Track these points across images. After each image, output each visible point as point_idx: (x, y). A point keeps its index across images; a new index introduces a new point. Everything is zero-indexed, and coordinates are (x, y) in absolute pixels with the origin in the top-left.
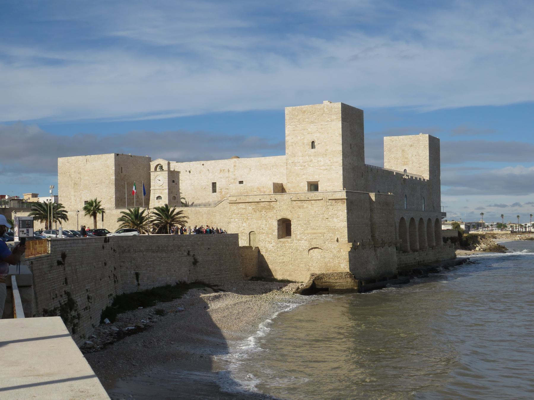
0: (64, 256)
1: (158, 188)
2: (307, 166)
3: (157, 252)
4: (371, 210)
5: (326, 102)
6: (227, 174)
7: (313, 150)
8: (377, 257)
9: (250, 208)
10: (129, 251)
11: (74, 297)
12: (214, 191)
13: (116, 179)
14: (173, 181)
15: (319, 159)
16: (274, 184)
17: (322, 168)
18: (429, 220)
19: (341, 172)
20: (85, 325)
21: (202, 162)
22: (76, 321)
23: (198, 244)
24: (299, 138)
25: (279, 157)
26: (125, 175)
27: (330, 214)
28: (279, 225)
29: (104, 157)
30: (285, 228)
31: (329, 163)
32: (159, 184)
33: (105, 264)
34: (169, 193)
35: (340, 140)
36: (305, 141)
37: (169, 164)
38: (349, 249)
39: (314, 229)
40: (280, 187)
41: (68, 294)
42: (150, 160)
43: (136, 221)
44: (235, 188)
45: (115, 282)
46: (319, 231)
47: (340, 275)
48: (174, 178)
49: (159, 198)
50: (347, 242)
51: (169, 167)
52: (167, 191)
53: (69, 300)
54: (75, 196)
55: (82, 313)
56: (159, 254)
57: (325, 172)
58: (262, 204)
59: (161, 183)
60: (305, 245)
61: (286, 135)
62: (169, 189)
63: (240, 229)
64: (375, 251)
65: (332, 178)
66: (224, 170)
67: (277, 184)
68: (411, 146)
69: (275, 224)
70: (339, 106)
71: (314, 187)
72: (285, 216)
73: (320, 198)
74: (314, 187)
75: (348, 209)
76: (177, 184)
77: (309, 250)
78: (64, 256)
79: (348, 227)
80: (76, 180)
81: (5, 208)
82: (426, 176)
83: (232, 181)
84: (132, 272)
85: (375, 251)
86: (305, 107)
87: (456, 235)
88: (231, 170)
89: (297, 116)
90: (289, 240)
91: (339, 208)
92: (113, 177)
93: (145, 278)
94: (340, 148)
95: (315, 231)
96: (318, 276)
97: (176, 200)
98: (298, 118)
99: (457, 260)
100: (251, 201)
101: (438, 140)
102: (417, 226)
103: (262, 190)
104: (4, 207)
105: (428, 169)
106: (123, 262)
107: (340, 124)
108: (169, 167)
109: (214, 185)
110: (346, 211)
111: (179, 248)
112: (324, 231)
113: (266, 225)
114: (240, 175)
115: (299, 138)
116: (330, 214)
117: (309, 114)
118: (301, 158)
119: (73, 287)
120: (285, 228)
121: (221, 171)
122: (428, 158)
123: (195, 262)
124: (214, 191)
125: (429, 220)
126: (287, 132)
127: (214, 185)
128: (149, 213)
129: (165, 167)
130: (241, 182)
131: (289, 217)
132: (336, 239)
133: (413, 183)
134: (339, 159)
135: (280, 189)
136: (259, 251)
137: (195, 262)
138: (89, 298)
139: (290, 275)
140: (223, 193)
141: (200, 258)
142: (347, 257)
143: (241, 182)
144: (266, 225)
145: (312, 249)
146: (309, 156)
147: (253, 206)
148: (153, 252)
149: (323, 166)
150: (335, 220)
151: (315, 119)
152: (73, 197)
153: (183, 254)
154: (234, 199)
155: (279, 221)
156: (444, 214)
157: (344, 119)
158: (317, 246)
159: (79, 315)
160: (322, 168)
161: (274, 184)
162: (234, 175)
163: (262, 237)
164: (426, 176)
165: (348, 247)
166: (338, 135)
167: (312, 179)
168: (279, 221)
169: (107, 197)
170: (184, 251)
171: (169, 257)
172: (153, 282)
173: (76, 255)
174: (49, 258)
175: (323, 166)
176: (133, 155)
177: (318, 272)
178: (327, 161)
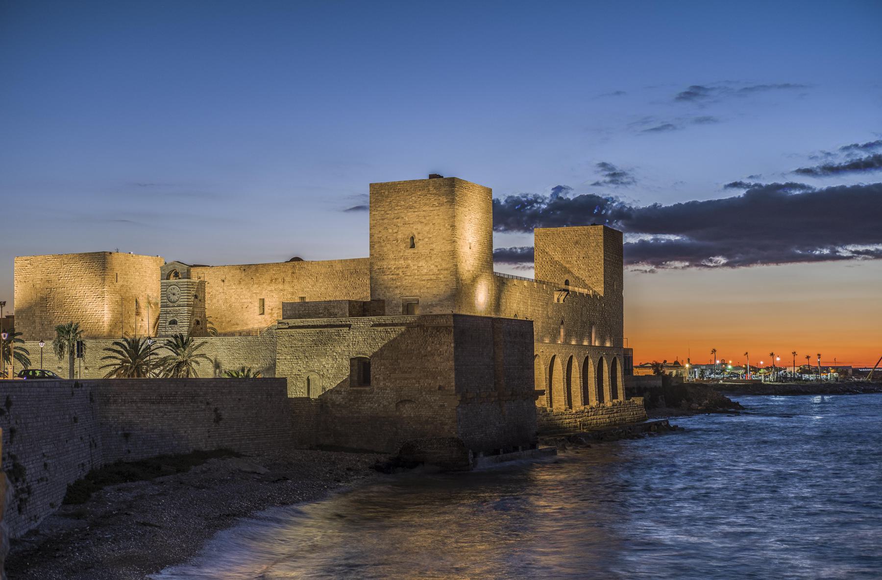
2: (401, 274)
7: (412, 251)
10: (115, 401)
11: (21, 462)
20: (39, 503)
22: (24, 496)
23: (222, 393)
24: (390, 231)
26: (122, 286)
28: (352, 365)
33: (76, 420)
36: (400, 236)
40: (360, 307)
41: (13, 457)
45: (91, 446)
53: (14, 465)
54: (41, 317)
55: (35, 486)
56: (162, 407)
66: (276, 279)
67: (356, 302)
68: (577, 243)
75: (456, 342)
79: (456, 369)
87: (659, 383)
89: (387, 197)
90: (367, 389)
95: (407, 375)
103: (332, 311)
110: (453, 345)
118: (393, 262)
123: (218, 419)
137: (218, 419)
138: (45, 465)
145: (401, 402)
146: (406, 259)
148: (153, 403)
150: (438, 359)
151: (416, 202)
152: (37, 320)
159: (28, 487)
170: (201, 402)
172: (152, 448)
178: (433, 267)
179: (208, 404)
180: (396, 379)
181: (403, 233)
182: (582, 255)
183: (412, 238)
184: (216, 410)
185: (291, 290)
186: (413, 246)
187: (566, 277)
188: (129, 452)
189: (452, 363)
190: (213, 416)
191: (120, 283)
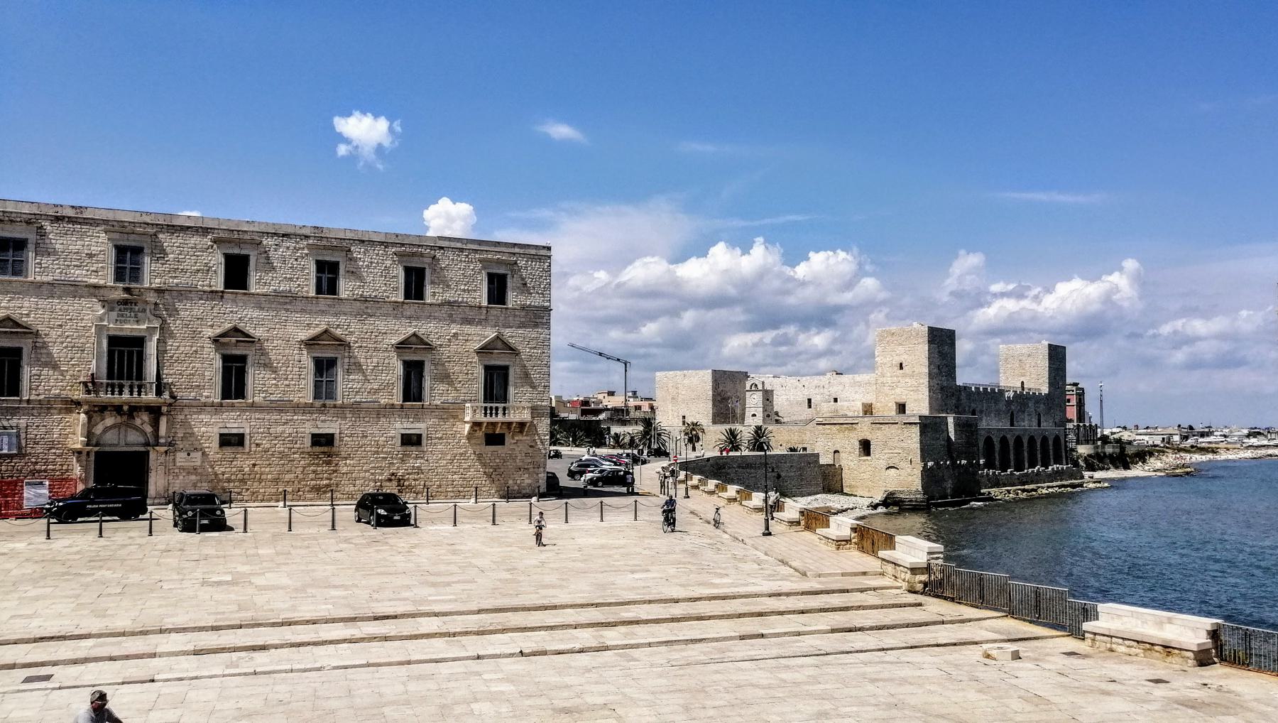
5: (915, 325)
9: (834, 428)
12: (810, 407)
29: (701, 373)
30: (866, 447)
34: (765, 410)
35: (926, 362)
42: (746, 376)
43: (732, 440)
44: (826, 409)
48: (768, 396)
60: (883, 464)
69: (857, 444)
71: (902, 408)
82: (1045, 390)
92: (711, 393)
102: (1026, 445)
109: (810, 400)
114: (835, 390)
120: (866, 447)
124: (810, 407)
127: (810, 400)
128: (745, 432)
129: (760, 387)
133: (1024, 399)
134: (925, 380)
137: (779, 476)
141: (783, 474)
157: (929, 342)
164: (1045, 390)
169: (702, 413)
181: (897, 360)
186: (901, 367)
187: (1022, 379)
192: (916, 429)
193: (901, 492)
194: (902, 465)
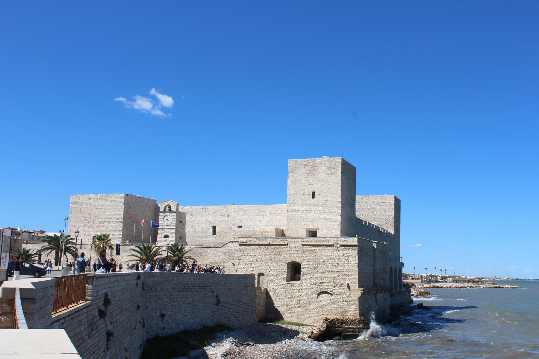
0: (107, 302)
1: (165, 227)
3: (183, 291)
4: (374, 258)
6: (226, 219)
8: (377, 302)
9: (259, 249)
10: (156, 289)
12: (214, 233)
13: (124, 217)
14: (181, 222)
15: (319, 208)
16: (276, 229)
17: (322, 216)
18: (396, 269)
19: (339, 221)
21: (204, 207)
25: (277, 205)
27: (341, 259)
28: (288, 268)
29: (114, 196)
30: (294, 271)
31: (328, 212)
32: (167, 224)
34: (177, 232)
35: (339, 191)
36: (306, 191)
37: (178, 205)
38: (360, 295)
39: (324, 273)
46: (329, 275)
47: (353, 321)
48: (181, 220)
49: (166, 236)
50: (357, 287)
51: (178, 209)
52: (174, 230)
57: (324, 220)
58: (272, 247)
59: (169, 223)
61: (288, 184)
62: (176, 228)
63: (249, 270)
64: (376, 296)
65: (330, 226)
66: (224, 215)
69: (285, 268)
70: (338, 161)
71: (313, 234)
72: (295, 260)
73: (331, 244)
74: (313, 234)
76: (184, 225)
77: (319, 294)
78: (107, 302)
80: (86, 216)
81: (17, 239)
82: (392, 231)
83: (232, 225)
84: (158, 313)
85: (376, 296)
86: (306, 160)
88: (231, 215)
91: (350, 255)
92: (122, 215)
93: (171, 321)
94: (340, 199)
95: (325, 276)
96: (332, 321)
97: (182, 240)
98: (300, 169)
99: (414, 304)
100: (261, 243)
101: (400, 201)
104: (15, 238)
105: (393, 225)
106: (150, 302)
107: (340, 178)
108: (178, 209)
109: (214, 228)
110: (357, 257)
111: (204, 287)
112: (333, 276)
113: (276, 267)
115: (300, 188)
116: (341, 259)
117: (311, 166)
119: (113, 352)
120: (294, 271)
121: (221, 216)
122: (393, 215)
123: (218, 303)
124: (214, 233)
125: (396, 269)
126: (289, 182)
127: (214, 228)
129: (174, 208)
130: (240, 227)
131: (299, 261)
132: (346, 284)
135: (281, 234)
136: (267, 293)
137: (218, 303)
139: (298, 318)
140: (222, 236)
141: (222, 300)
142: (358, 303)
143: (240, 227)
144: (276, 267)
147: (263, 248)
148: (180, 291)
149: (323, 214)
150: (346, 266)
153: (207, 294)
154: (245, 240)
155: (288, 264)
156: (403, 264)
157: (343, 173)
158: (327, 290)
160: (322, 216)
161: (276, 229)
162: (234, 220)
163: (270, 279)
164: (392, 231)
165: (357, 292)
166: (337, 187)
167: (312, 227)
168: (288, 264)
170: (209, 291)
171: (194, 297)
172: (178, 325)
173: (117, 298)
174: (89, 309)
175: (323, 214)
176: (141, 196)
177: (331, 317)
179: (212, 292)
180: (318, 278)
182: (382, 211)
183: (314, 194)
184: (217, 296)
185: (233, 222)
188: (164, 328)
189: (357, 269)
190: (215, 301)
191: (132, 212)
192: (354, 253)
193: (343, 321)
194: (337, 290)
